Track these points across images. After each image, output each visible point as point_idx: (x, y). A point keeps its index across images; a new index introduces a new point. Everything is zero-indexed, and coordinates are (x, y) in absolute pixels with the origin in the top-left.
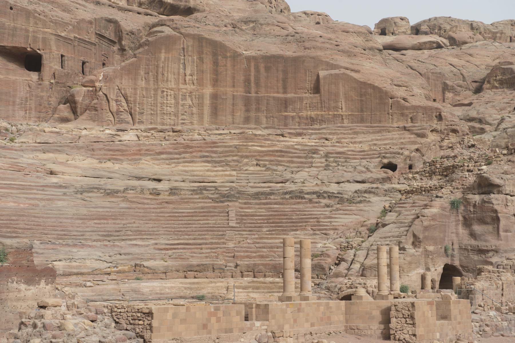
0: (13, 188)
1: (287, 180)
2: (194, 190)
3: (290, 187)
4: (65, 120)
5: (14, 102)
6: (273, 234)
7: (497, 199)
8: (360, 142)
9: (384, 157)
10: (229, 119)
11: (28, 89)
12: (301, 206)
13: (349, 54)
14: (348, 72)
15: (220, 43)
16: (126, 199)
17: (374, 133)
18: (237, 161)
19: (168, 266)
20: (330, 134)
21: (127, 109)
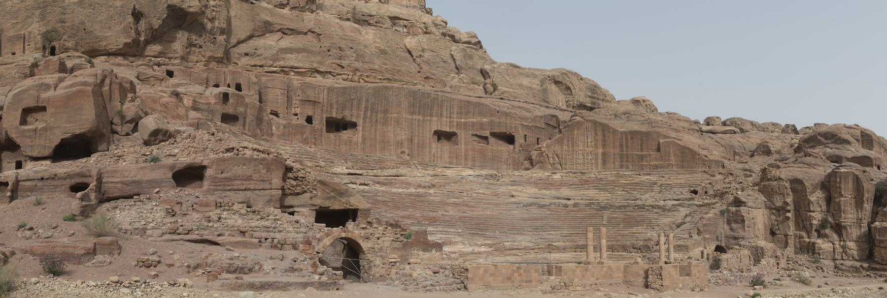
4: (527, 169)
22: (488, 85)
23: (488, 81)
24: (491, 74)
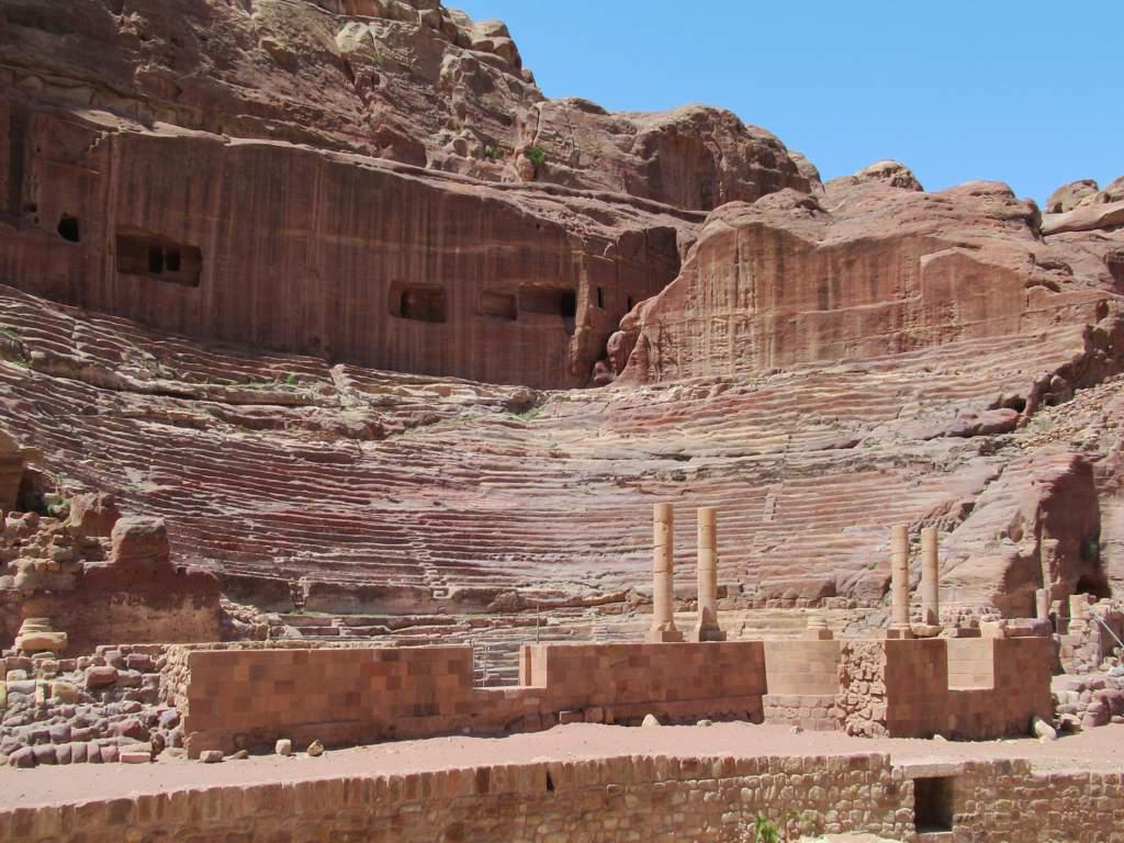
12: (870, 483)
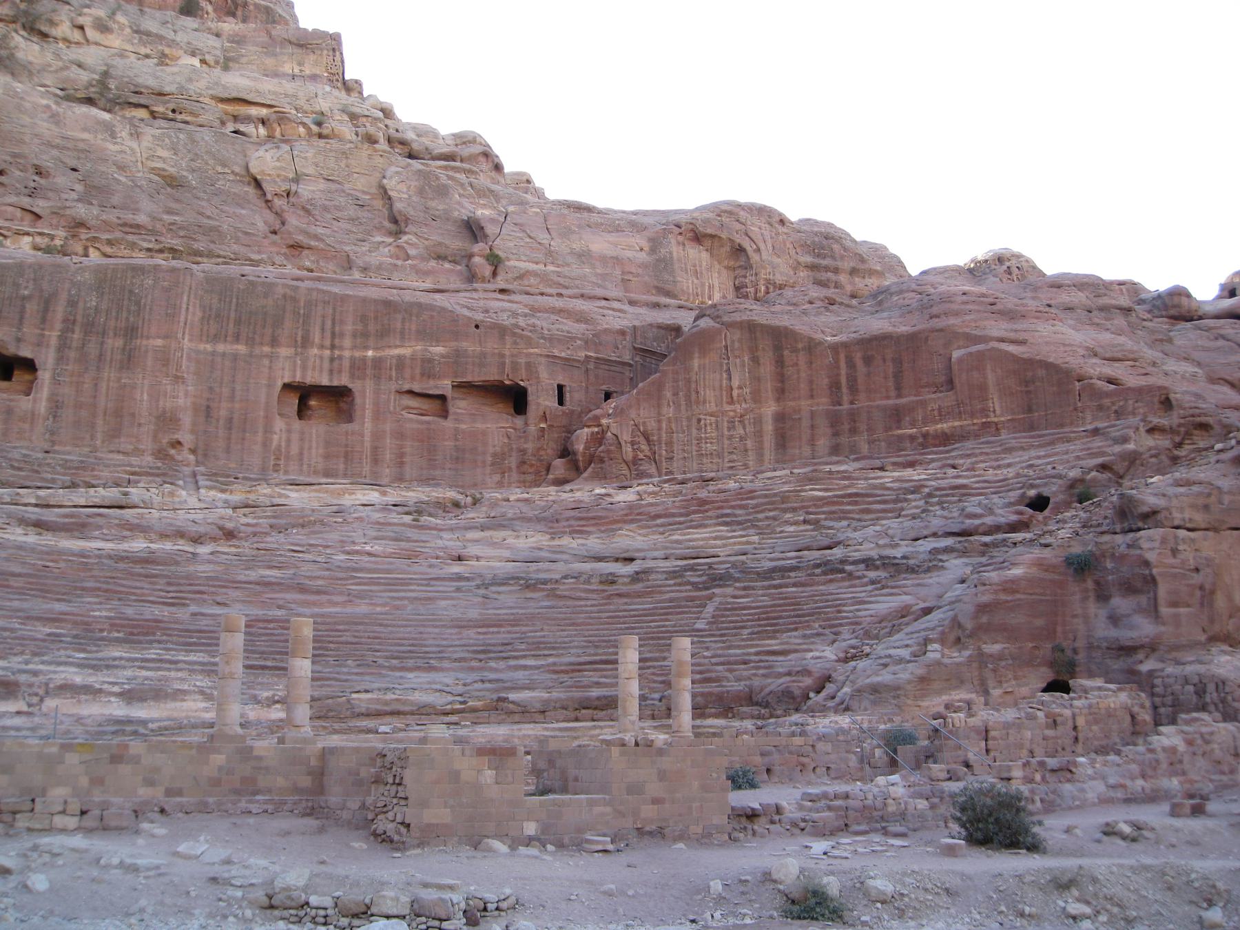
0: (379, 584)
1: (838, 543)
2: (674, 572)
3: (838, 552)
4: (560, 482)
5: (484, 462)
6: (753, 639)
7: (1151, 540)
8: (1009, 465)
9: (1032, 486)
10: (807, 451)
11: (506, 441)
12: (832, 588)
13: (1010, 315)
14: (1004, 346)
15: (786, 328)
16: (553, 594)
17: (1040, 446)
18: (774, 519)
19: (547, 701)
20: (962, 457)
21: (648, 454)
22: (477, 260)
23: (479, 247)
24: (491, 230)
